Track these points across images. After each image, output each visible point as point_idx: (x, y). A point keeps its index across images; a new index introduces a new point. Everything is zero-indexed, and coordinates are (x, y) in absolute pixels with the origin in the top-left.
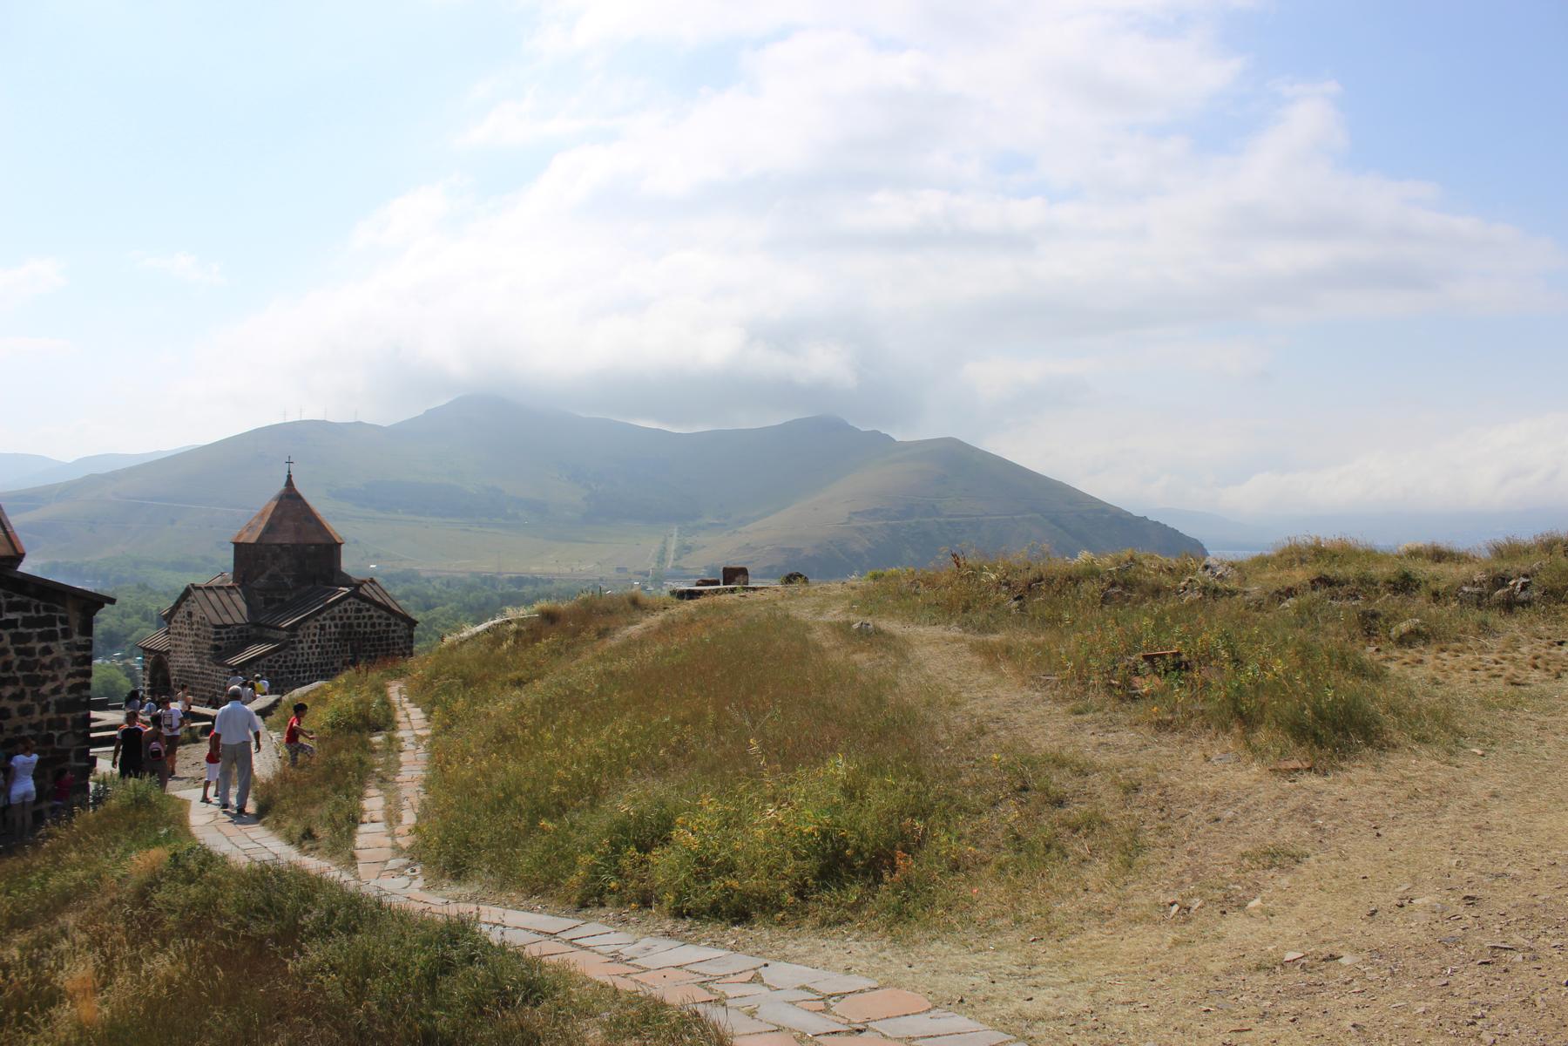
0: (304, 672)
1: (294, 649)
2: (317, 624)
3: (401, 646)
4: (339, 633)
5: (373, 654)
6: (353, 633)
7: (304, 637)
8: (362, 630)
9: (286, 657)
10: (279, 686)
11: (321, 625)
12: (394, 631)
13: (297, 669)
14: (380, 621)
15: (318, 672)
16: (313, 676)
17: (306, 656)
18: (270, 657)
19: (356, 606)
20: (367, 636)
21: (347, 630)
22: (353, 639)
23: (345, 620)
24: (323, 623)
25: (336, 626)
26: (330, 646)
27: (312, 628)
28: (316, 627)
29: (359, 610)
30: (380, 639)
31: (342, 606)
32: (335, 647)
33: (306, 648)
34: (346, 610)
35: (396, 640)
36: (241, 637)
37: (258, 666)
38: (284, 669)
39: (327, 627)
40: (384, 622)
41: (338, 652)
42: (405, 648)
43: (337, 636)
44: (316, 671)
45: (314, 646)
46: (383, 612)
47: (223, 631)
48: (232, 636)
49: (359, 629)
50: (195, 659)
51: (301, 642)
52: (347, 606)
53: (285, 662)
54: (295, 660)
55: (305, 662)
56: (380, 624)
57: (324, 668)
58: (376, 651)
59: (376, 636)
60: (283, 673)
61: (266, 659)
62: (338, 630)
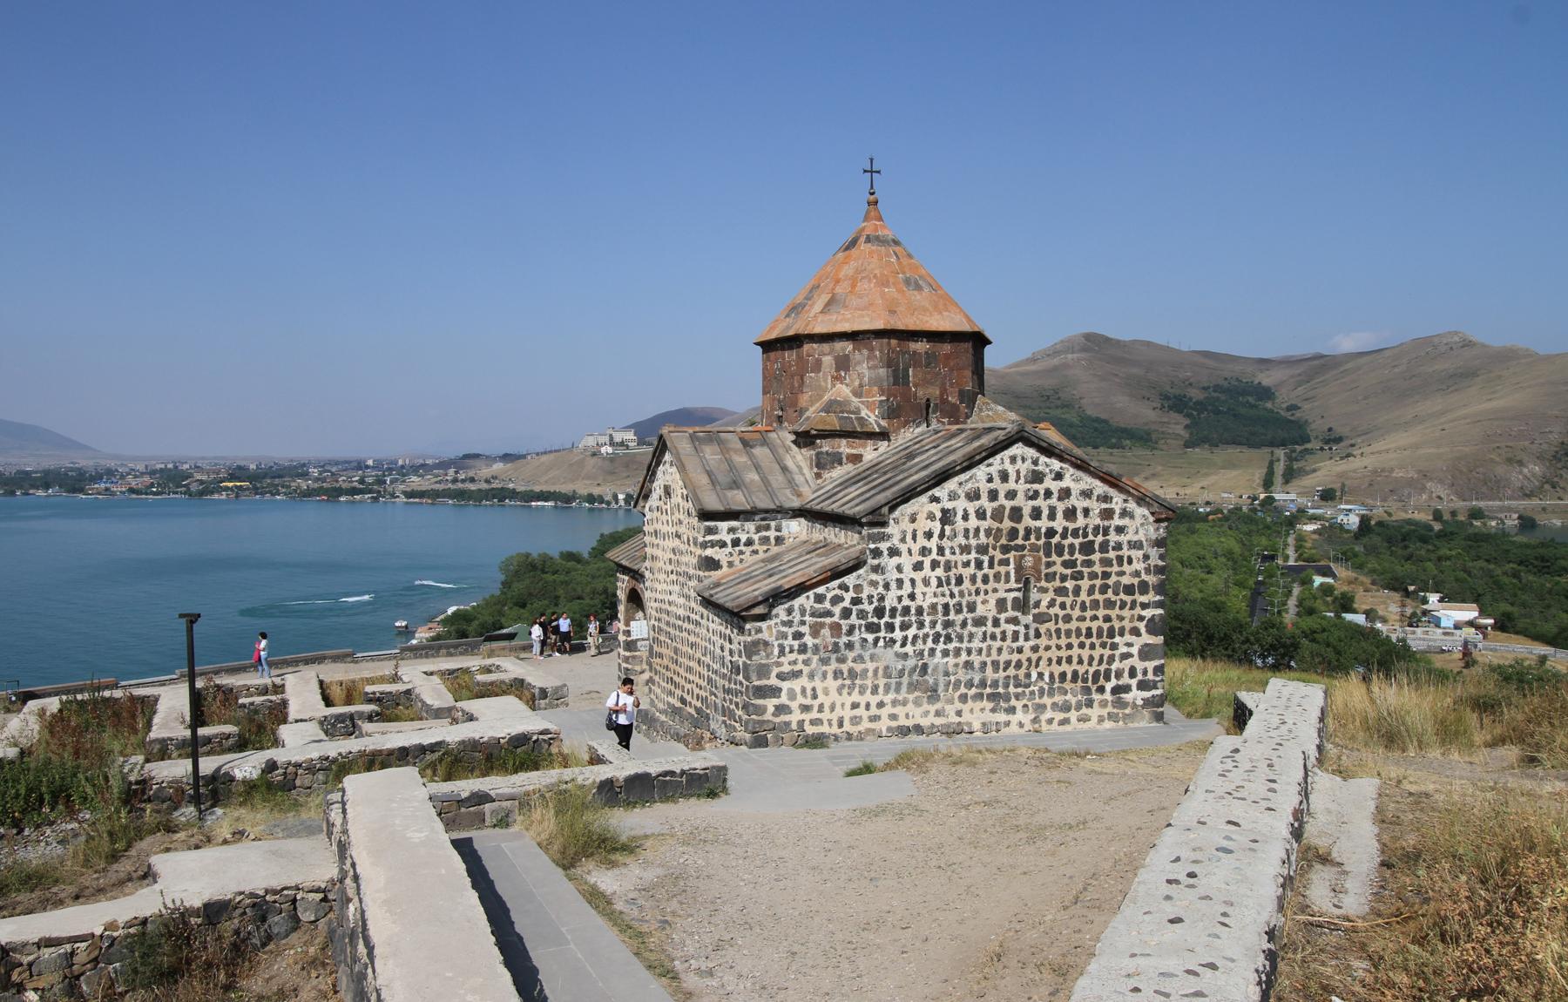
0: (904, 627)
1: (876, 569)
2: (936, 508)
4: (988, 532)
6: (1022, 533)
7: (903, 540)
8: (1043, 524)
9: (858, 588)
10: (842, 660)
11: (944, 512)
12: (1120, 530)
13: (886, 619)
14: (1086, 503)
15: (939, 628)
16: (926, 636)
17: (907, 584)
19: (1028, 465)
20: (1055, 540)
21: (1007, 524)
22: (1023, 548)
24: (949, 505)
25: (981, 515)
26: (967, 564)
27: (921, 517)
28: (931, 517)
30: (1087, 548)
32: (979, 565)
33: (908, 568)
34: (1004, 477)
35: (1125, 552)
37: (790, 611)
38: (853, 619)
39: (960, 514)
40: (1096, 507)
41: (985, 580)
42: (1148, 571)
43: (983, 539)
44: (934, 624)
45: (927, 564)
47: (724, 526)
48: (744, 538)
49: (1038, 523)
50: (676, 588)
51: (894, 552)
53: (856, 601)
54: (882, 599)
55: (906, 602)
56: (1086, 512)
57: (952, 616)
59: (1077, 542)
60: (851, 631)
61: (811, 593)
62: (984, 525)
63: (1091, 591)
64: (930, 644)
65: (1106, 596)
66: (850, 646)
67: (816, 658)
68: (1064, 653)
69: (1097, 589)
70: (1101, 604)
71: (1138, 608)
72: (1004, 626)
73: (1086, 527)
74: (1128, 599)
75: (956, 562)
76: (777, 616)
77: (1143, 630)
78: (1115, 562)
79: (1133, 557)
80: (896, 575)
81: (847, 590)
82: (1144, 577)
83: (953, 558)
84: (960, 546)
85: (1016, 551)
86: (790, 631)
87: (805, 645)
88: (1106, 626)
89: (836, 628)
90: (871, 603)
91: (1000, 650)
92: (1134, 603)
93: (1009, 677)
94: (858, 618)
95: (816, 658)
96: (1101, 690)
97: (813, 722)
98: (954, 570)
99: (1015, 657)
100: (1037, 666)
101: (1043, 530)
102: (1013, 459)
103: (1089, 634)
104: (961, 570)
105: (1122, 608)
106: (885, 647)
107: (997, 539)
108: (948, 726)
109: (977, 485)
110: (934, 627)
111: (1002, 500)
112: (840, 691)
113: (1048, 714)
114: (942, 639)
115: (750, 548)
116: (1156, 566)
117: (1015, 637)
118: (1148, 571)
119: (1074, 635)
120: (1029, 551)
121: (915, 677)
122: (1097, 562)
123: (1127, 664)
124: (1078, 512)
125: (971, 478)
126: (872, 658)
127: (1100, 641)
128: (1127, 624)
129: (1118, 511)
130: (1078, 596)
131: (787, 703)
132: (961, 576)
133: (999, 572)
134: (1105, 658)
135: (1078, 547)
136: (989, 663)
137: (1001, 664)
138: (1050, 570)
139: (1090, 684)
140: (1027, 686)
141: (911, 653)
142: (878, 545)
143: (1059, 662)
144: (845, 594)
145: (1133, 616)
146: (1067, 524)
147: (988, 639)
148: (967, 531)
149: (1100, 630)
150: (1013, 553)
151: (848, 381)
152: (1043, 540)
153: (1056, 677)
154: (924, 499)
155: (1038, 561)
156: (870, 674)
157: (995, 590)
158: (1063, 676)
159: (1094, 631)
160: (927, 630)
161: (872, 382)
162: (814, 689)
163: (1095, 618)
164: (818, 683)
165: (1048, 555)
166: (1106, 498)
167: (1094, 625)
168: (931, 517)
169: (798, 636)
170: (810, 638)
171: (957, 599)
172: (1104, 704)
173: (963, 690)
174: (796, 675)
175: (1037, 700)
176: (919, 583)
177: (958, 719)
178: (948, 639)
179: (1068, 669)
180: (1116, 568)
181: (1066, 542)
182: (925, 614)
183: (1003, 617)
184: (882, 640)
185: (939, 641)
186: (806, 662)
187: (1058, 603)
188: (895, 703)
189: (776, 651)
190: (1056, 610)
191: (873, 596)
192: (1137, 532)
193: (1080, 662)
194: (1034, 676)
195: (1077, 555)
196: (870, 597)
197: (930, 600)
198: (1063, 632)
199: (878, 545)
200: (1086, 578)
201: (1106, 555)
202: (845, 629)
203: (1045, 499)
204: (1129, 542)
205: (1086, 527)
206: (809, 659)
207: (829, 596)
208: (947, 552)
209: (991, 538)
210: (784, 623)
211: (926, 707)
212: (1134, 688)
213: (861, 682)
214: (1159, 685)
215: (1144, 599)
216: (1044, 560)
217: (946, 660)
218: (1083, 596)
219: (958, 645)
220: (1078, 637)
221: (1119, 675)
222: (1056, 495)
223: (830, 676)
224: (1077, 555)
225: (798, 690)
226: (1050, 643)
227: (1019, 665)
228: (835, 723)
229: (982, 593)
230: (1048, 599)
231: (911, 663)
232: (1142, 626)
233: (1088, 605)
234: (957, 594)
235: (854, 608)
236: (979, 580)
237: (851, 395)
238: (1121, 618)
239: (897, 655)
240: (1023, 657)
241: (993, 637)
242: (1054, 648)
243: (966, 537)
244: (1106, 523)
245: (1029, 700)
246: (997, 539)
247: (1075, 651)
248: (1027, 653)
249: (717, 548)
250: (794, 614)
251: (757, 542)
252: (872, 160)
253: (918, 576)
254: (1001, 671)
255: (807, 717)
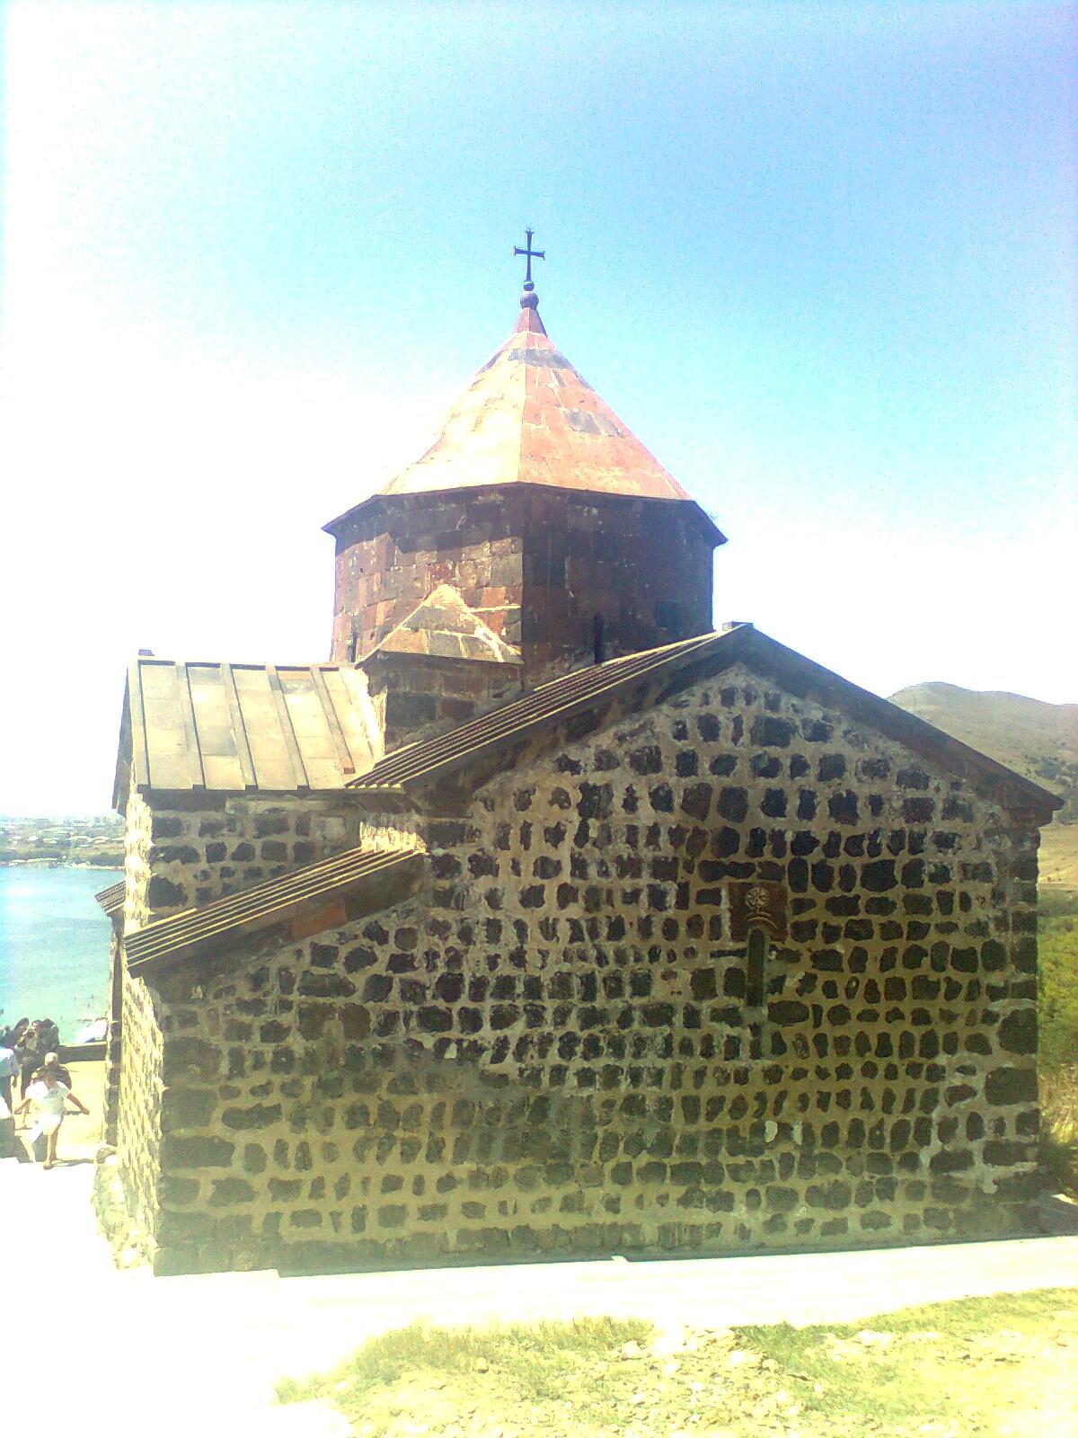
0: (501, 1020)
1: (445, 898)
2: (568, 782)
3: (979, 912)
4: (676, 835)
5: (839, 947)
7: (502, 843)
8: (788, 825)
9: (406, 936)
11: (584, 788)
12: (944, 842)
13: (464, 1001)
14: (875, 788)
15: (573, 1024)
16: (546, 1041)
17: (509, 935)
18: (327, 938)
20: (815, 856)
22: (747, 869)
23: (705, 773)
24: (596, 778)
25: (661, 800)
26: (632, 897)
28: (560, 798)
29: (775, 732)
30: (879, 876)
31: (693, 704)
33: (511, 900)
34: (709, 728)
35: (956, 885)
36: (275, 851)
38: (394, 1002)
40: (897, 796)
41: (670, 929)
42: (1001, 923)
43: (666, 848)
44: (562, 1016)
45: (551, 893)
46: (895, 749)
47: (194, 820)
48: (232, 844)
49: (778, 823)
51: (483, 866)
52: (715, 705)
53: (399, 963)
54: (455, 959)
55: (505, 968)
56: (876, 803)
57: (600, 1001)
58: (859, 931)
59: (858, 863)
60: (388, 1023)
62: (672, 819)
63: (887, 961)
64: (553, 1057)
65: (920, 972)
66: (385, 1056)
67: (309, 1081)
68: (833, 1086)
69: (899, 957)
70: (909, 987)
71: (985, 997)
72: (709, 1026)
73: (876, 833)
74: (962, 978)
75: (610, 893)
76: (230, 990)
77: (994, 1041)
78: (935, 905)
79: (972, 895)
80: (484, 912)
81: (382, 938)
82: (994, 934)
83: (604, 883)
84: (619, 859)
85: (733, 875)
86: (256, 1022)
87: (288, 1053)
88: (918, 1032)
89: (356, 1020)
90: (432, 967)
91: (700, 1075)
92: (975, 984)
93: (717, 1131)
94: (404, 997)
95: (309, 1081)
96: (911, 1162)
97: (298, 1218)
98: (606, 909)
99: (732, 1091)
100: (777, 1109)
101: (789, 837)
102: (728, 697)
103: (884, 1048)
104: (621, 909)
105: (950, 996)
106: (459, 1061)
107: (695, 848)
108: (590, 1230)
109: (655, 743)
110: (563, 1023)
111: (705, 773)
112: (359, 1152)
113: (802, 1212)
114: (579, 1049)
115: (245, 865)
116: (1018, 914)
117: (733, 1047)
118: (1001, 923)
119: (852, 1049)
120: (760, 876)
121: (522, 1121)
122: (900, 905)
123: (962, 1105)
124: (859, 804)
125: (642, 728)
126: (432, 1083)
127: (906, 1062)
128: (959, 1026)
129: (940, 806)
130: (862, 969)
131: (244, 1175)
132: (620, 920)
133: (698, 916)
134: (918, 1097)
135: (859, 873)
136: (677, 1102)
137: (703, 1102)
138: (805, 917)
139: (887, 1150)
140: (757, 1151)
141: (514, 1075)
142: (453, 851)
143: (823, 1102)
144: (378, 951)
145: (972, 1013)
146: (837, 827)
147: (676, 1050)
148: (632, 830)
149: (906, 1037)
150: (727, 879)
151: (457, 578)
152: (789, 856)
153: (818, 1132)
154: (548, 764)
155: (777, 898)
156: (426, 1118)
157: (690, 953)
158: (831, 1131)
159: (895, 1042)
160: (547, 1029)
161: (499, 577)
162: (304, 1148)
163: (895, 1015)
164: (312, 1135)
165: (799, 886)
166: (917, 780)
167: (895, 1031)
168: (560, 798)
169: (274, 1032)
170: (299, 1037)
171: (612, 966)
172: (915, 1191)
173: (623, 1158)
174: (264, 1116)
175: (778, 1183)
176: (533, 931)
177: (607, 1218)
178: (593, 1048)
179: (843, 1119)
180: (936, 917)
181: (836, 863)
182: (545, 994)
183: (706, 1006)
184: (453, 1047)
185: (573, 1053)
186: (290, 1090)
187: (820, 983)
188: (476, 1179)
189: (224, 1067)
190: (817, 996)
191: (436, 955)
192: (978, 848)
193: (867, 1104)
194: (771, 1129)
195: (858, 889)
196: (431, 956)
197: (556, 966)
198: (830, 1042)
199: (453, 851)
200: (877, 936)
201: (918, 891)
202: (374, 1022)
203: (792, 777)
204: (964, 866)
205: (876, 833)
206: (296, 1082)
207: (344, 952)
208: (592, 870)
209: (683, 848)
210: (246, 1006)
211: (543, 1190)
212: (978, 1158)
213: (408, 1135)
214: (1031, 1153)
215: (996, 979)
216: (791, 895)
217: (586, 1093)
218: (872, 970)
219: (612, 1061)
220: (861, 1053)
221: (946, 1130)
222: (813, 771)
223: (339, 1121)
224: (858, 889)
225: (269, 1148)
226: (805, 1065)
227: (739, 1107)
228: (347, 1220)
229: (663, 956)
230: (801, 975)
231: (513, 1095)
232: (992, 1033)
233: (881, 988)
234: (611, 954)
235: (397, 977)
236: (657, 930)
237: (461, 602)
238: (949, 1017)
239: (485, 1077)
240: (749, 1091)
241: (686, 1048)
242: (812, 1075)
243: (632, 841)
244: (917, 828)
245: (760, 1180)
246: (695, 848)
247: (856, 1082)
248: (757, 1083)
249: (178, 862)
250: (267, 986)
251: (258, 852)
252: (530, 235)
253: (532, 917)
254: (702, 1119)
255: (286, 1207)
